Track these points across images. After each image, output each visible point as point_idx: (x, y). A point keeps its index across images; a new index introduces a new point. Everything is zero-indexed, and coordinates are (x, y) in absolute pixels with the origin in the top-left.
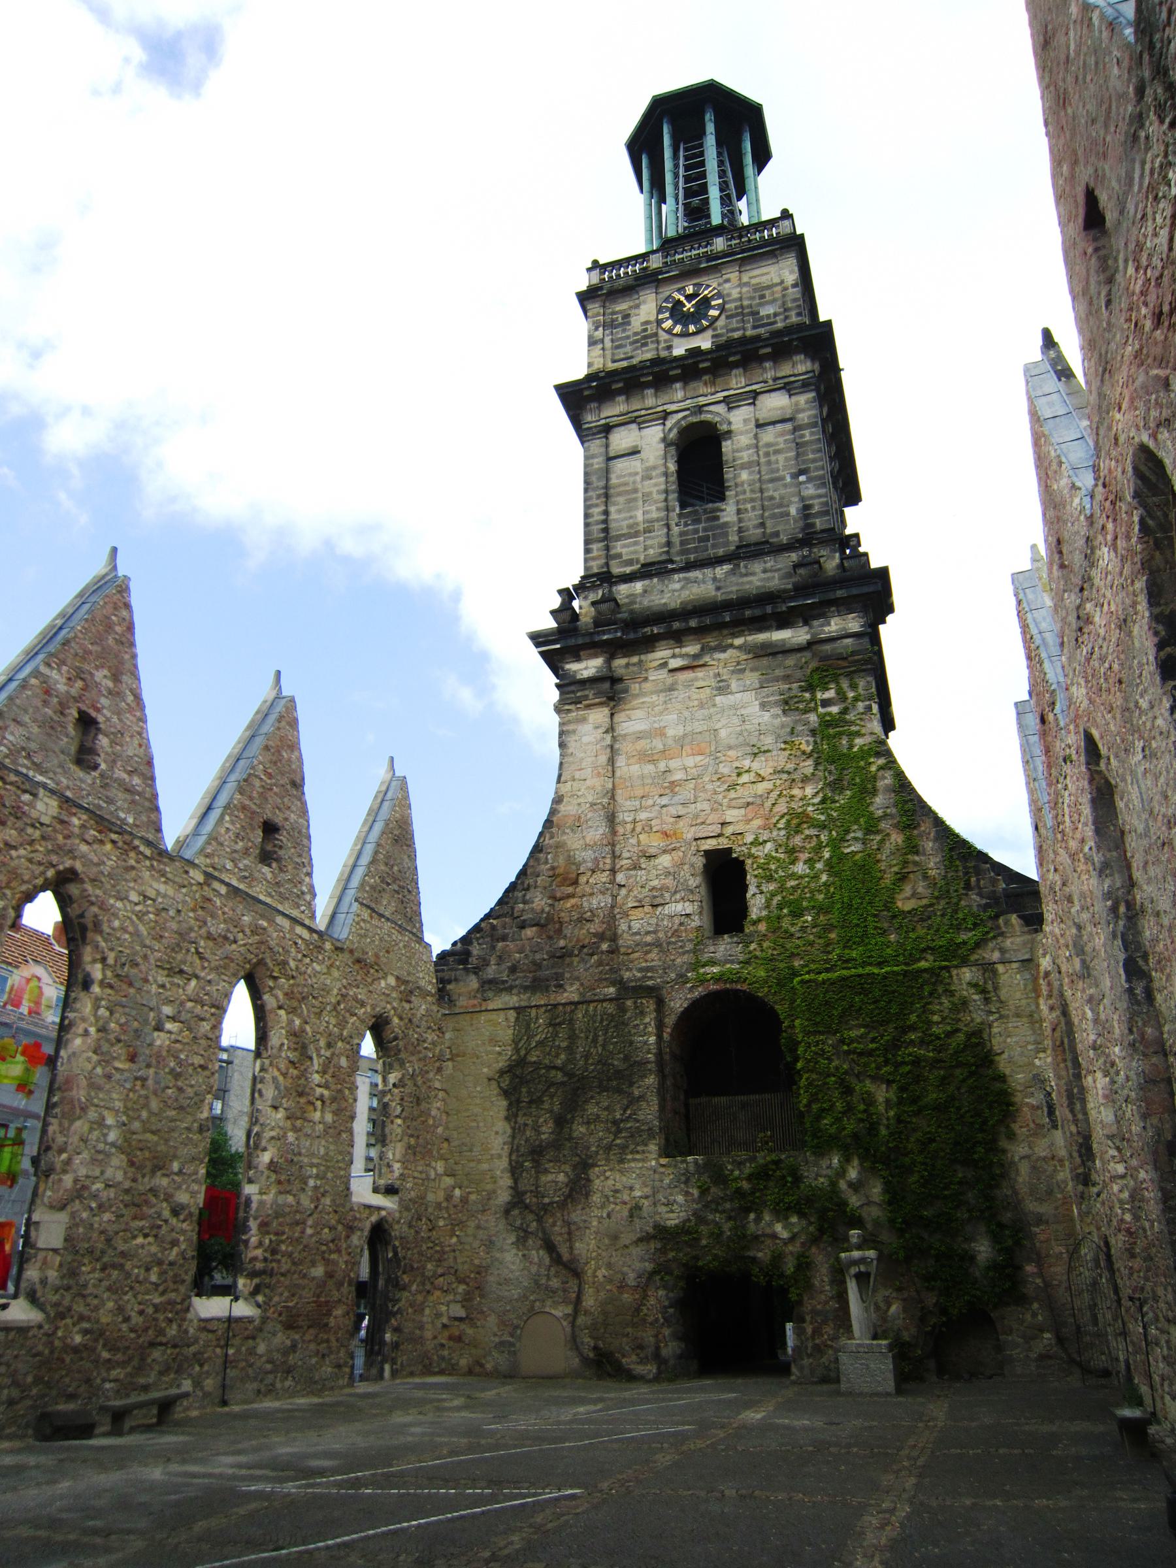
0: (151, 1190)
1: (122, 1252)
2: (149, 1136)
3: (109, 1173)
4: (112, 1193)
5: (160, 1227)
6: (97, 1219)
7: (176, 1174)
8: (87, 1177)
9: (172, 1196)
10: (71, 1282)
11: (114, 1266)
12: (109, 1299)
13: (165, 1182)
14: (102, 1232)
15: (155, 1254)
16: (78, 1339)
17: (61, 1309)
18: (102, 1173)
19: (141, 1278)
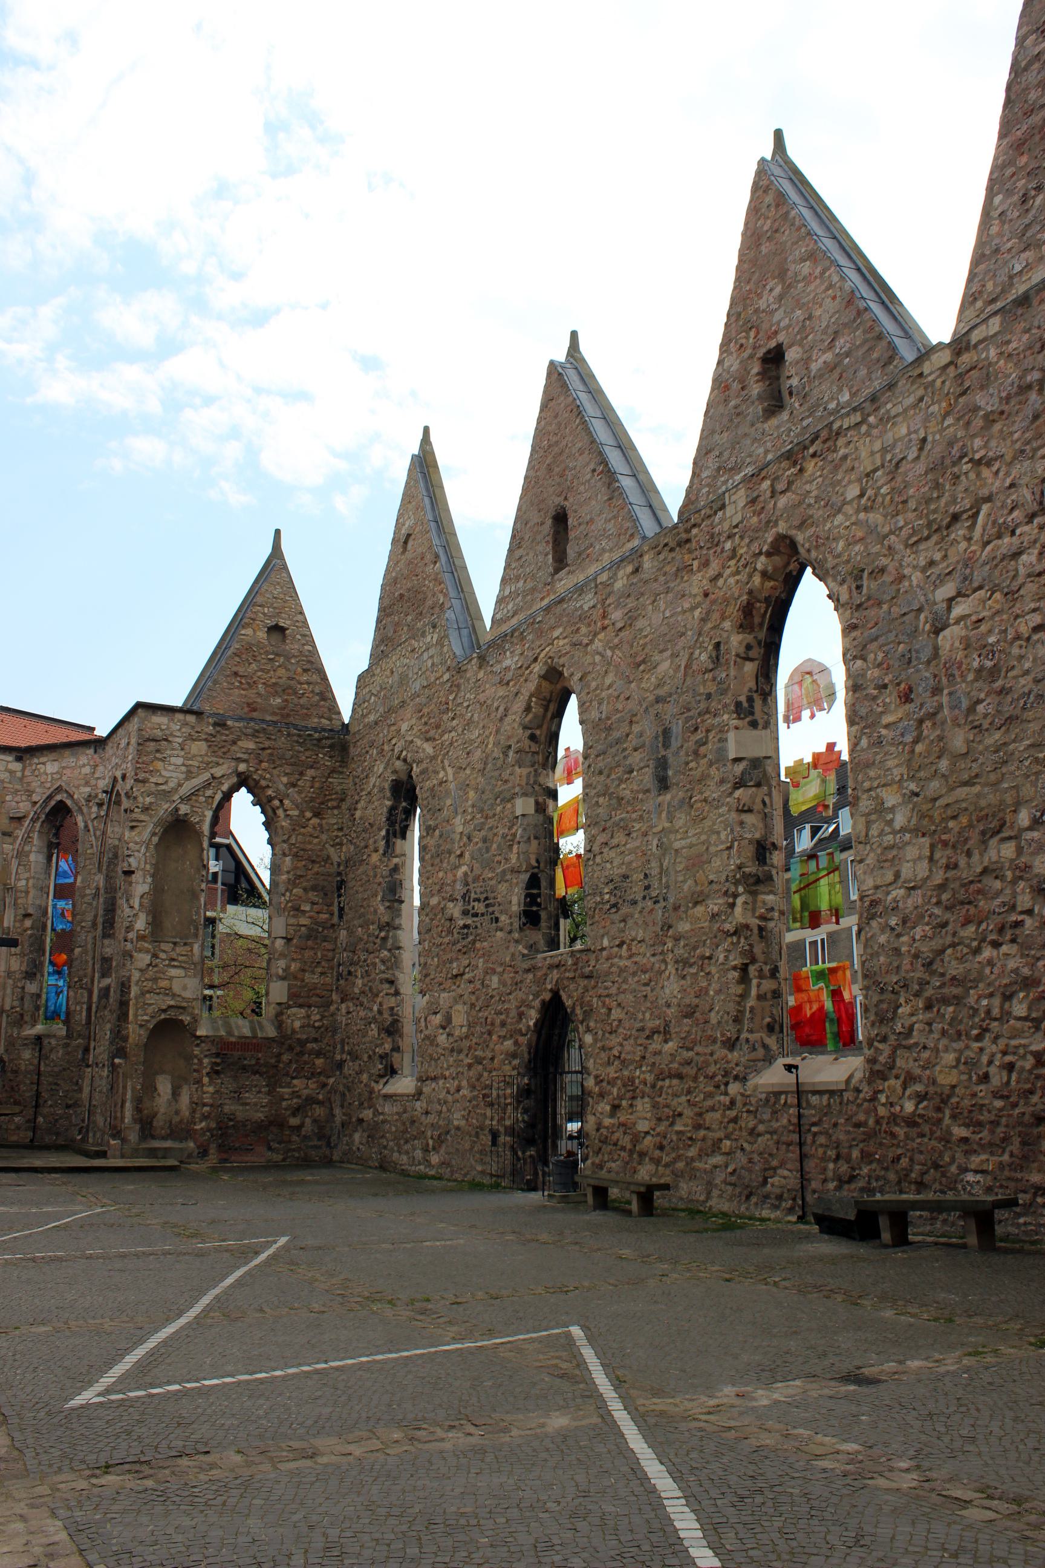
0: (985, 871)
1: (954, 978)
2: (962, 792)
3: (906, 871)
4: (917, 898)
5: (1018, 924)
6: (904, 939)
7: (1030, 829)
8: (877, 888)
9: (1028, 867)
10: (884, 1030)
11: (945, 1001)
12: (946, 1050)
13: (1008, 850)
14: (916, 956)
15: (1016, 971)
16: (909, 1107)
17: (877, 1067)
18: (897, 875)
19: (996, 1012)
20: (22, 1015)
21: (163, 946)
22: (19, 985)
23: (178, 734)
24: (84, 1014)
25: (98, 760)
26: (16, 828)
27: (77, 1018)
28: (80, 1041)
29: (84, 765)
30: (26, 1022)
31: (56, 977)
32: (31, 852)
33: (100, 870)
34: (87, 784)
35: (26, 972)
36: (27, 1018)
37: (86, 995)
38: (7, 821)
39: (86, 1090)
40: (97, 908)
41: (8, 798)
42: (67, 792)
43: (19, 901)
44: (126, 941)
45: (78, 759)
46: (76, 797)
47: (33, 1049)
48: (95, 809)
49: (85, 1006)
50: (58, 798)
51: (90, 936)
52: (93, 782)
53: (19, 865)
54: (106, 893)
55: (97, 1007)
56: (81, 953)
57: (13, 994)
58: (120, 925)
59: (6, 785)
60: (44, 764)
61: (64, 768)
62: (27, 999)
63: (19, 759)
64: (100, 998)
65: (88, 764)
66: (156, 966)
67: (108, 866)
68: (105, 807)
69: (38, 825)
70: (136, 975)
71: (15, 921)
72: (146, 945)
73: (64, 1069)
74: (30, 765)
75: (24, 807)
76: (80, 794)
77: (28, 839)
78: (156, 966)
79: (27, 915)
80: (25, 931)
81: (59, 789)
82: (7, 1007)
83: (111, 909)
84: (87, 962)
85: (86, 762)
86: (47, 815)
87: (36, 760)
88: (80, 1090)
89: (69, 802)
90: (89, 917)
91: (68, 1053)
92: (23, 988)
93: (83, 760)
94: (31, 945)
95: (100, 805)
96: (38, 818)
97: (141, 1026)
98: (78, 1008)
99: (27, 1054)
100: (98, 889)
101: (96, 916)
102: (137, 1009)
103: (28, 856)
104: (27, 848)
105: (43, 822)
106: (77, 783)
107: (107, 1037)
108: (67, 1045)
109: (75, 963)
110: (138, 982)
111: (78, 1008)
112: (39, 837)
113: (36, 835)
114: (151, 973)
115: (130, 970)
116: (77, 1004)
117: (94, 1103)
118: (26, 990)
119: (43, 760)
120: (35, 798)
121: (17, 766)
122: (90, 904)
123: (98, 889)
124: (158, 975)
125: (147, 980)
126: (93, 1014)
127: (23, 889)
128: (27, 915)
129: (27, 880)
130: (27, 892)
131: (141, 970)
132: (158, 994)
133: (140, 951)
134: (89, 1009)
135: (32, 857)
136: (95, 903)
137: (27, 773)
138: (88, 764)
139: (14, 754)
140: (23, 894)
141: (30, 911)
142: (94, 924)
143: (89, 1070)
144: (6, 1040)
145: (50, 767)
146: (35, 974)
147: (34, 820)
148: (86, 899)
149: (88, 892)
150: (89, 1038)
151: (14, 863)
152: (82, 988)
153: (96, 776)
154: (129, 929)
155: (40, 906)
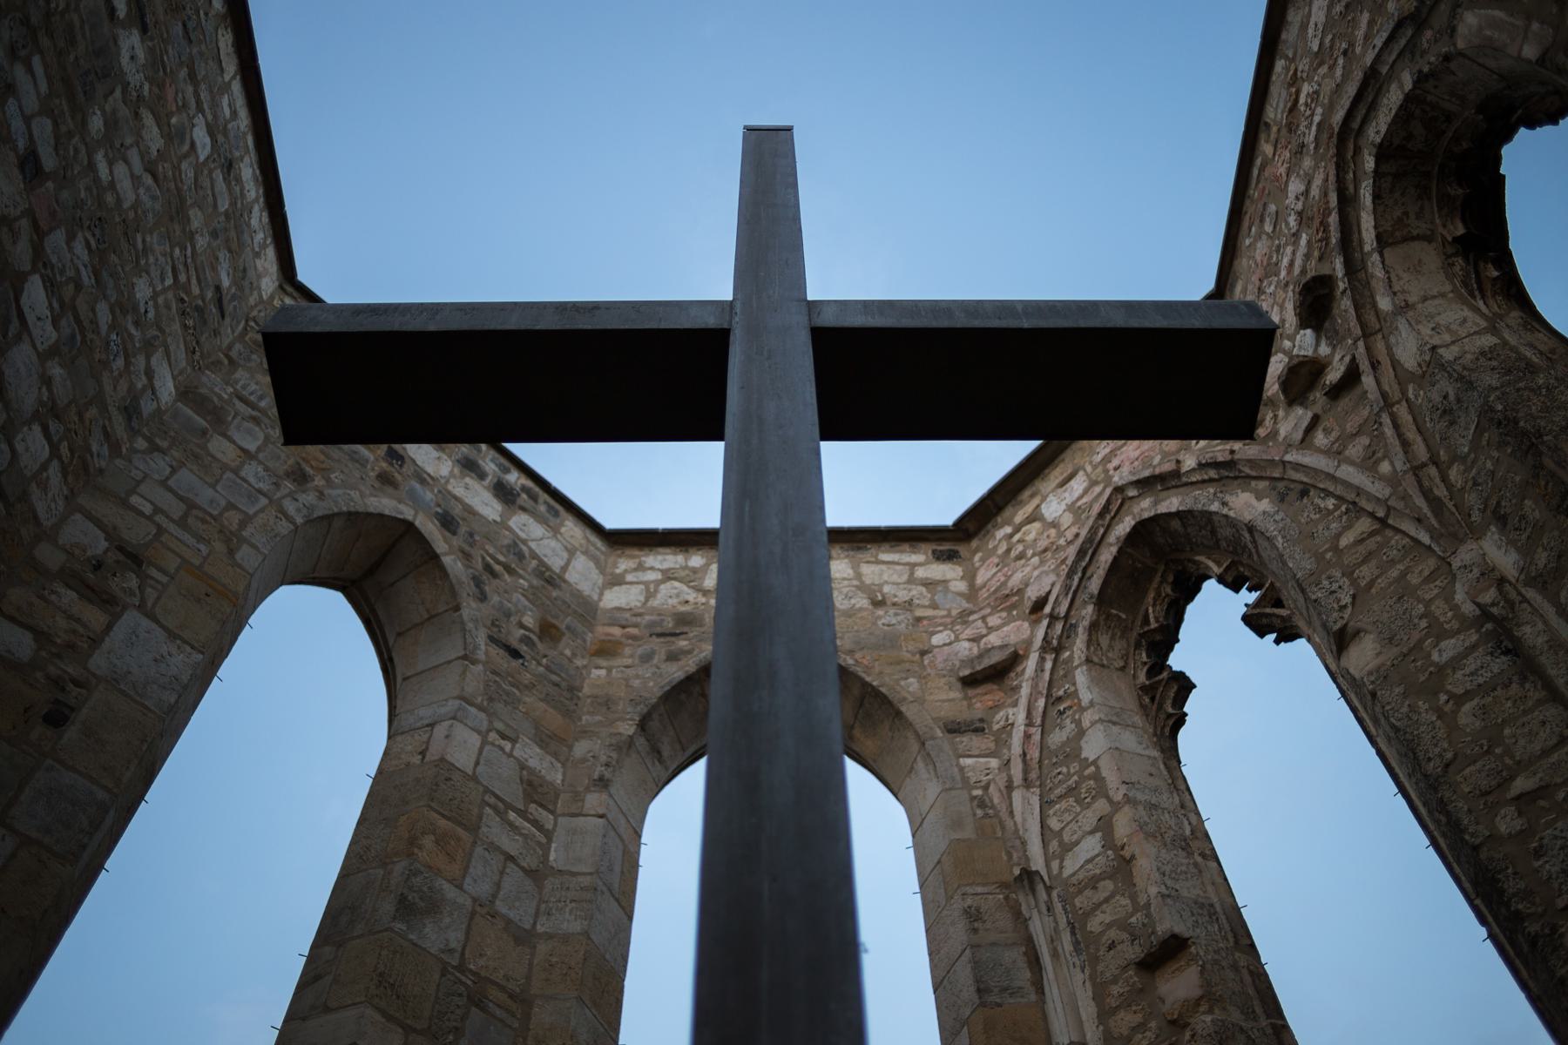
38: (956, 694)
53: (1045, 804)
69: (1078, 647)
86: (1101, 600)
87: (1000, 534)
96: (1069, 630)
105: (1093, 627)
112: (1095, 681)
113: (1081, 677)
139: (929, 548)
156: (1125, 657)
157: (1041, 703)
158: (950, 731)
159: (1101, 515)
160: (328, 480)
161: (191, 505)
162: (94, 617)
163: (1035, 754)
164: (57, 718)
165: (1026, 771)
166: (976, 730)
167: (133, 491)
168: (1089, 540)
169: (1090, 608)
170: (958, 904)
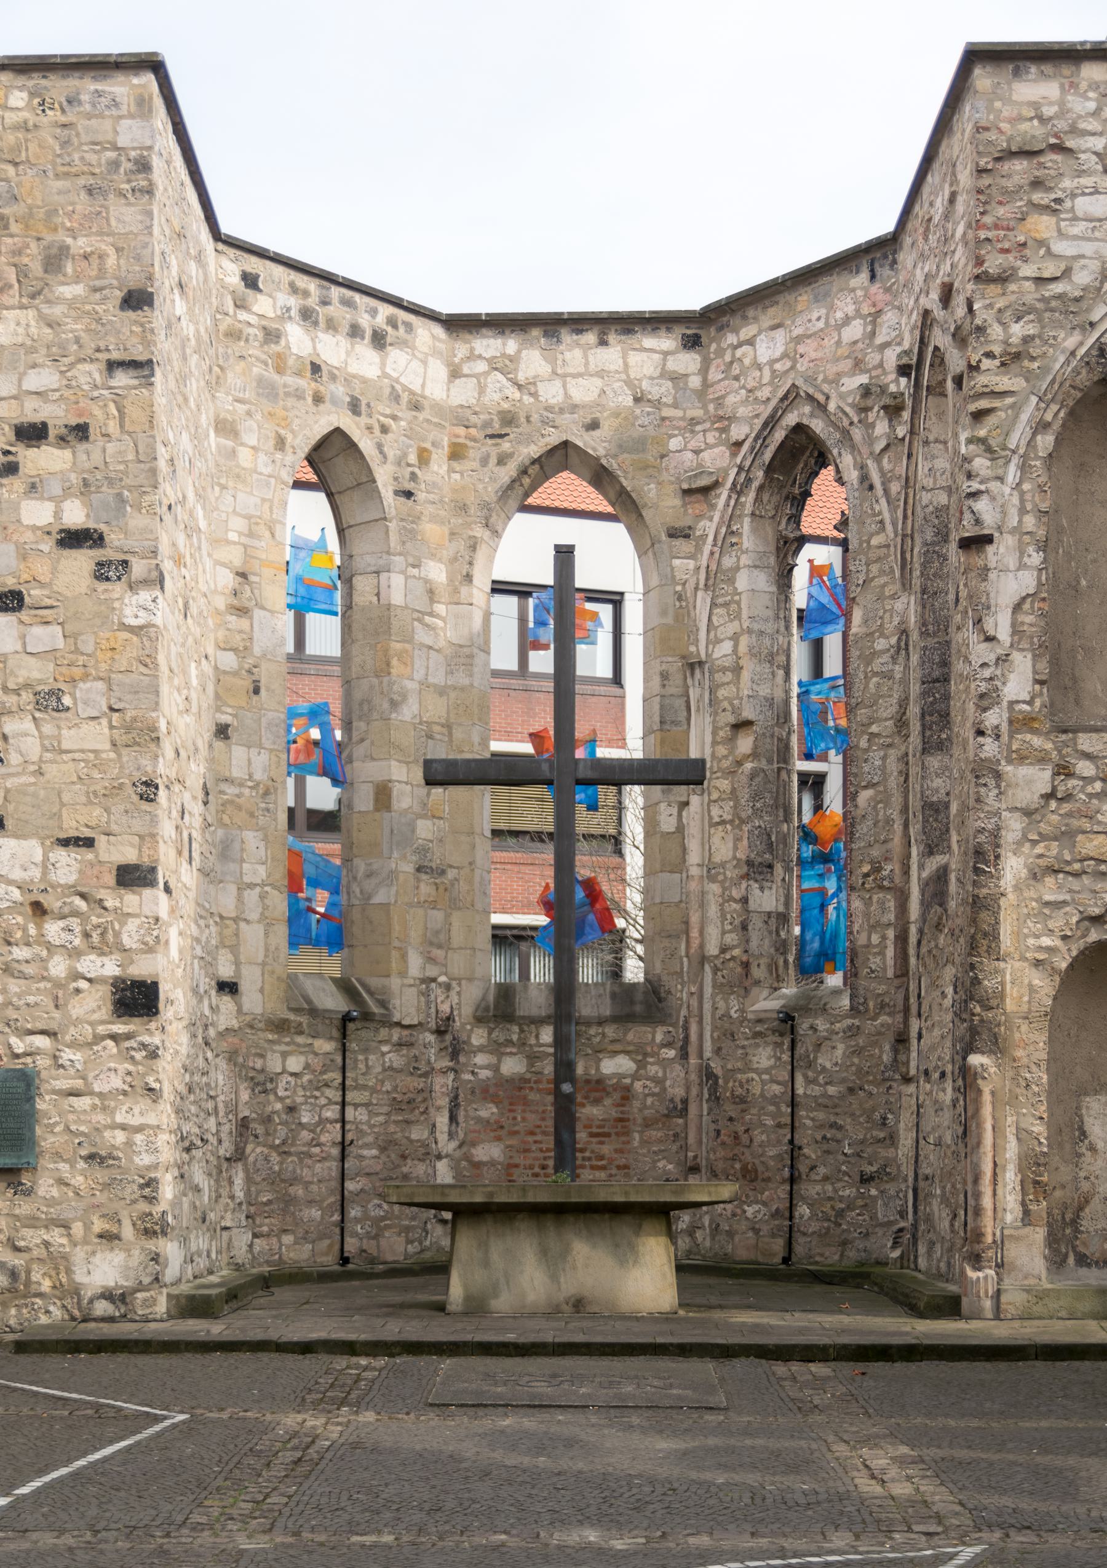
20: (746, 965)
21: (1086, 742)
22: (736, 893)
23: (1093, 125)
24: (890, 952)
25: (881, 297)
26: (699, 517)
27: (875, 962)
28: (884, 1019)
29: (847, 320)
30: (757, 983)
31: (820, 868)
32: (737, 569)
33: (906, 585)
34: (858, 365)
35: (749, 863)
36: (758, 973)
37: (891, 904)
38: (678, 502)
39: (906, 1140)
40: (905, 682)
41: (674, 444)
42: (810, 398)
43: (722, 693)
44: (980, 733)
45: (831, 308)
46: (832, 407)
47: (777, 1045)
48: (881, 428)
49: (891, 933)
50: (791, 419)
51: (893, 754)
52: (873, 358)
53: (714, 605)
54: (924, 634)
55: (921, 931)
56: (874, 802)
57: (723, 917)
58: (963, 711)
59: (667, 412)
60: (751, 342)
61: (799, 340)
62: (756, 923)
63: (692, 343)
64: (925, 905)
65: (858, 314)
66: (1068, 797)
67: (924, 565)
68: (906, 415)
69: (749, 499)
70: (1014, 827)
71: (714, 743)
72: (1037, 741)
73: (851, 1090)
74: (720, 352)
75: (716, 458)
76: (842, 396)
77: (728, 539)
78: (1068, 797)
79: (741, 726)
80: (739, 763)
81: (791, 397)
82: (712, 949)
83: (938, 678)
84: (889, 821)
85: (850, 309)
86: (770, 469)
87: (731, 339)
88: (892, 1139)
89: (818, 426)
90: (888, 709)
91: (858, 1051)
92: (745, 900)
93: (845, 306)
94: (755, 796)
95: (893, 411)
96: (749, 480)
97: (1038, 963)
98: (875, 939)
99: (764, 1057)
100: (904, 632)
101: (903, 703)
102: (1022, 920)
103: (732, 581)
104: (728, 562)
105: (761, 488)
106: (832, 370)
107: (948, 1002)
108: (853, 1032)
109: (862, 829)
110: (1019, 843)
111: (875, 939)
112: (754, 530)
113: (746, 526)
114: (1053, 819)
115: (997, 813)
116: (873, 928)
117: (926, 1170)
118: (752, 905)
119: (746, 332)
120: (738, 432)
121: (688, 362)
122: (888, 676)
123: (904, 632)
124: (1075, 823)
125: (1043, 837)
126: (912, 951)
127: (728, 662)
128: (741, 726)
129: (735, 638)
130: (737, 669)
131: (1028, 813)
132: (1076, 875)
133: (1022, 759)
134: (902, 939)
135: (743, 582)
136: (898, 669)
137: (714, 375)
138: (858, 314)
139: (680, 330)
140: (729, 676)
141: (748, 714)
142: (901, 723)
143: (911, 1089)
144: (715, 1028)
145: (765, 346)
146: (770, 866)
147: (738, 490)
148: (877, 665)
149: (881, 644)
150: (906, 1010)
151: (703, 601)
152: (881, 888)
153: (879, 340)
154: (987, 700)
155: (770, 701)
156: (776, 508)
157: (724, 530)
158: (671, 535)
159: (782, 400)
160: (293, 432)
161: (248, 517)
162: (244, 623)
163: (713, 567)
164: (256, 691)
165: (707, 579)
166: (687, 536)
167: (227, 530)
168: (772, 416)
169: (760, 474)
170: (657, 667)
